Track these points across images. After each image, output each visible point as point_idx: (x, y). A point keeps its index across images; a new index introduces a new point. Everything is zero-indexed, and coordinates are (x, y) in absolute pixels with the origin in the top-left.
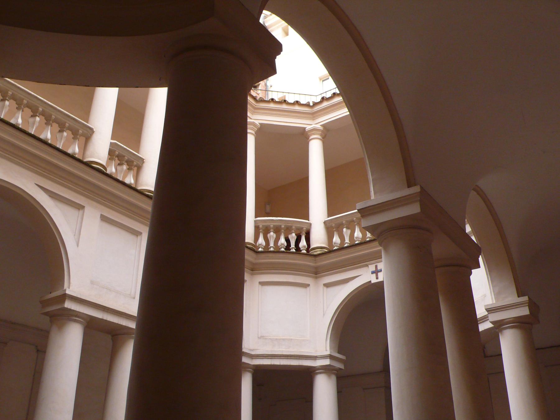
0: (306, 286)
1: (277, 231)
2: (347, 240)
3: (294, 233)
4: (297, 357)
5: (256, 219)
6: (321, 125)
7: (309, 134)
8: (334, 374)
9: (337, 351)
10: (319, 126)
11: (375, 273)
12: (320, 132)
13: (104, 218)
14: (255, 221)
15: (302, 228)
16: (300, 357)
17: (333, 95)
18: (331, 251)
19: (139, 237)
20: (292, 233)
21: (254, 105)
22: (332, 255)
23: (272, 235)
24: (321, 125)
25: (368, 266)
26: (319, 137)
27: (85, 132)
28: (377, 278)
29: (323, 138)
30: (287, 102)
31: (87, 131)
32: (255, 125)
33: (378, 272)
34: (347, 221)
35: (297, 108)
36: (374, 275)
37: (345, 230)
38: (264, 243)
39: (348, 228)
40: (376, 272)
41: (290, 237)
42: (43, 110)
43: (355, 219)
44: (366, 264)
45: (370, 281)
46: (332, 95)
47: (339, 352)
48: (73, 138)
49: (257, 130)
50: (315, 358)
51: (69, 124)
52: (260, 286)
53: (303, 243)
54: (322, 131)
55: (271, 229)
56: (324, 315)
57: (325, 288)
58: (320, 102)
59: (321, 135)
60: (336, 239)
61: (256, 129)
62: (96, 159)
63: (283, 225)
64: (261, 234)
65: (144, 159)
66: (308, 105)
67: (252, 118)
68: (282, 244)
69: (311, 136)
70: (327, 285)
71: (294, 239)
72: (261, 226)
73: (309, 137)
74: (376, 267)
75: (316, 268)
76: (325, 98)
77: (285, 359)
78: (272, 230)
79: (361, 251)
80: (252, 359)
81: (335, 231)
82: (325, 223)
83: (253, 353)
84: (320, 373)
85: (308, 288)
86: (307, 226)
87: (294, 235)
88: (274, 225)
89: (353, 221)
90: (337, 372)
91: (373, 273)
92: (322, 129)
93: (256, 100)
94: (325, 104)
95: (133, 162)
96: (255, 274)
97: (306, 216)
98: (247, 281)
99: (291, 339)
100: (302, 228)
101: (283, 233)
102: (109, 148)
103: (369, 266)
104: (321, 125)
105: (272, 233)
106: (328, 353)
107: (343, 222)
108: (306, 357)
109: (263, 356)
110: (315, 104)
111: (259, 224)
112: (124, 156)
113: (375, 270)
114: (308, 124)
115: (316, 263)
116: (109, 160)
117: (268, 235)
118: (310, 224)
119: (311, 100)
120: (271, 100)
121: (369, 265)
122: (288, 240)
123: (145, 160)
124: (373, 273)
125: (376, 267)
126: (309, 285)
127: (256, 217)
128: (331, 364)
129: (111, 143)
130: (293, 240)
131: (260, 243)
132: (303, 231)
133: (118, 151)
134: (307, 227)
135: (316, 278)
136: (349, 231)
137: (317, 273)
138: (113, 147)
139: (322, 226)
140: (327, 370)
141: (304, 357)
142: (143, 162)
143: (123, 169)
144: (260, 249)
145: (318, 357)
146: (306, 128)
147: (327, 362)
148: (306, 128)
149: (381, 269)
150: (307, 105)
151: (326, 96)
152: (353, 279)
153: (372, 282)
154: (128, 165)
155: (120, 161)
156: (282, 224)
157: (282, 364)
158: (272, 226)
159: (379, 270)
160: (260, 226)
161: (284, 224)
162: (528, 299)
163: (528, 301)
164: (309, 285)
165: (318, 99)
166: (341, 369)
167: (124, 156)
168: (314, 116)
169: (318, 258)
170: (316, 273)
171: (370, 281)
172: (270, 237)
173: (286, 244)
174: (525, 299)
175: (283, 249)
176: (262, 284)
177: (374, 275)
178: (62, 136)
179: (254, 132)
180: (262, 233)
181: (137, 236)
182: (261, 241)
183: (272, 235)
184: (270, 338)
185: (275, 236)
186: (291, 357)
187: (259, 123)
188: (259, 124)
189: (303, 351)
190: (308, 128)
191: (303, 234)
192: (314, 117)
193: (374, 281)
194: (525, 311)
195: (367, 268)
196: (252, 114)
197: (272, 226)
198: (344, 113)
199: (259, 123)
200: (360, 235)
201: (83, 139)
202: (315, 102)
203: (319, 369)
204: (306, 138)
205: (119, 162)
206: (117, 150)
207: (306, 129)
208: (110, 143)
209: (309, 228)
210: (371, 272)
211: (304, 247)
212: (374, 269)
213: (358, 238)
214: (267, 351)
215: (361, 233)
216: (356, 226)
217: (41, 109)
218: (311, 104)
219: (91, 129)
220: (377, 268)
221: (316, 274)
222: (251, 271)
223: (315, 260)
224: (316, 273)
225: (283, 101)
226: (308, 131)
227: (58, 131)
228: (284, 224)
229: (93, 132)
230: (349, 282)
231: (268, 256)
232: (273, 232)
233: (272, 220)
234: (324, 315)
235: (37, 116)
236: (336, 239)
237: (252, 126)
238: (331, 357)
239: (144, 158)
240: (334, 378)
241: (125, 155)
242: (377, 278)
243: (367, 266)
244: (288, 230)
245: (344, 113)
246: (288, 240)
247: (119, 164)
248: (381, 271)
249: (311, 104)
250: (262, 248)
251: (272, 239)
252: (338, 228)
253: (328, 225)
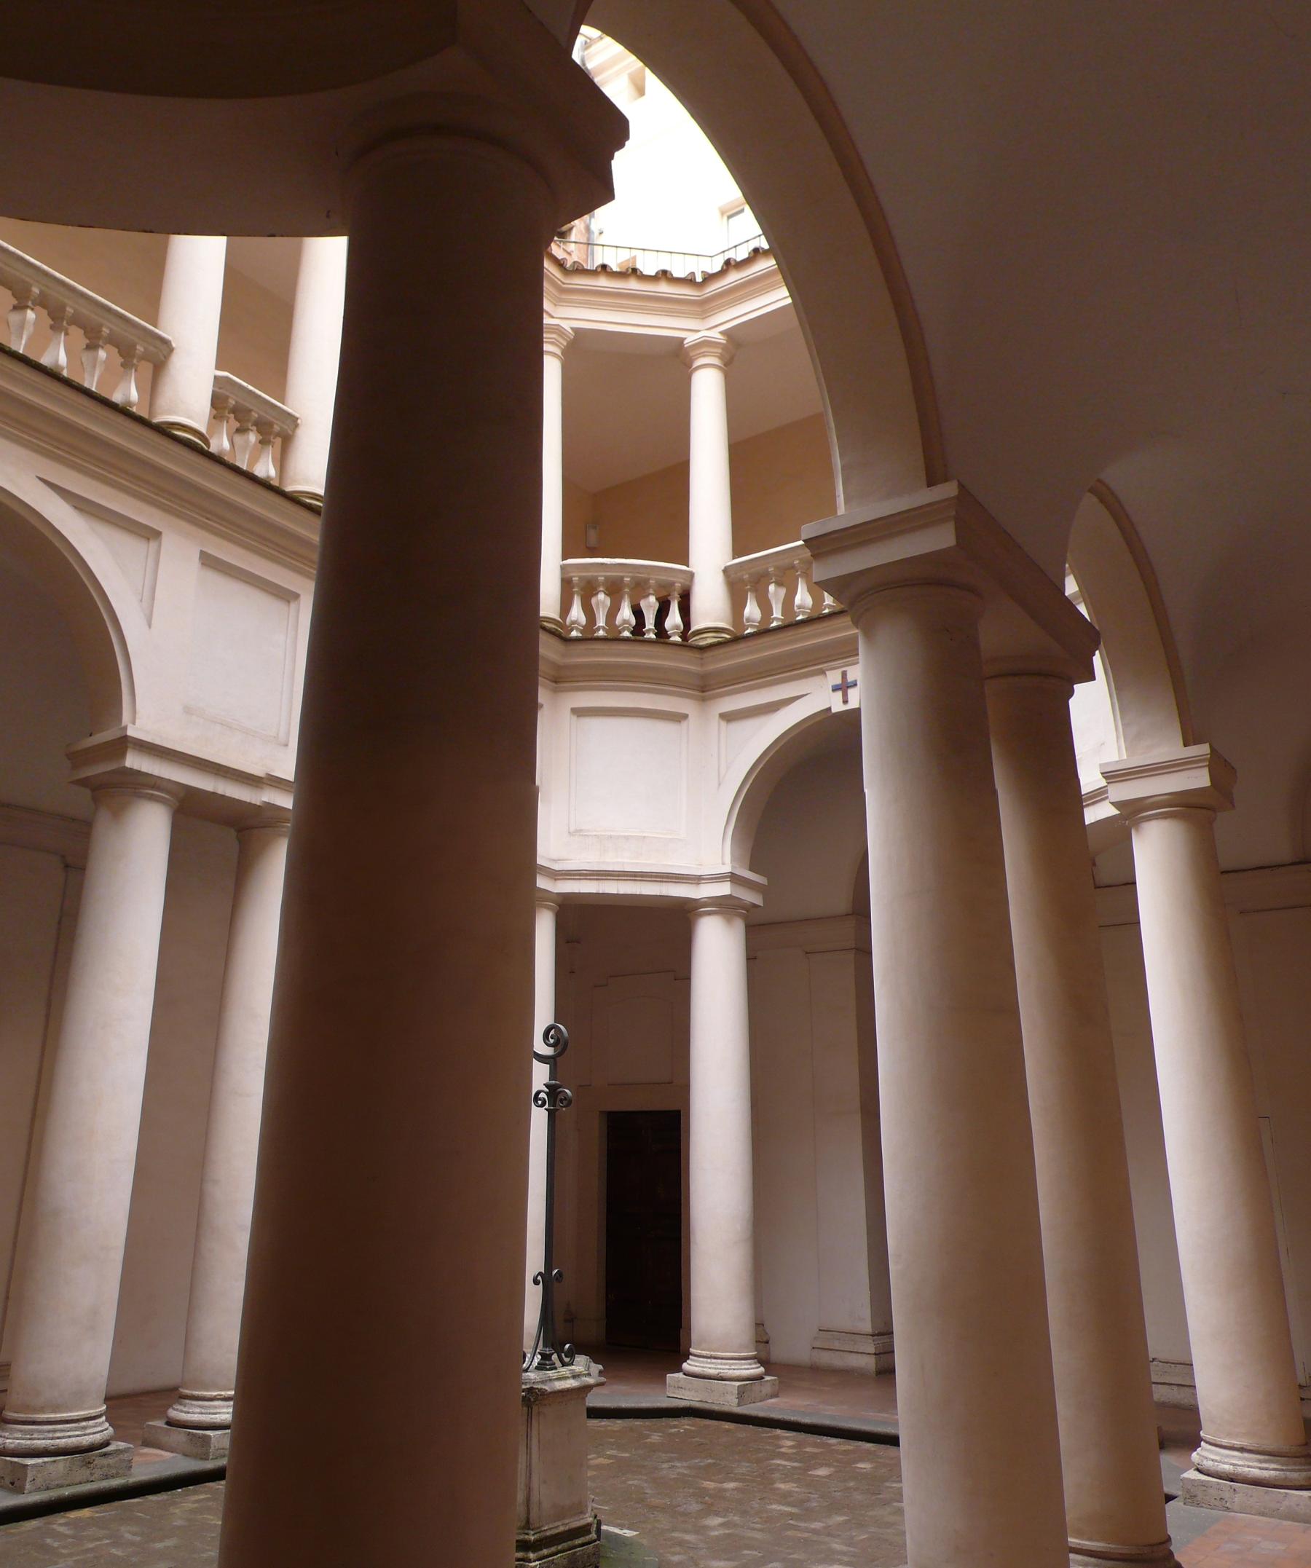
0: (679, 718)
1: (614, 590)
2: (777, 613)
3: (652, 594)
4: (656, 877)
5: (565, 562)
6: (721, 333)
7: (691, 354)
8: (740, 915)
9: (748, 867)
10: (715, 335)
12: (720, 351)
13: (208, 561)
14: (563, 568)
15: (672, 584)
16: (662, 877)
17: (752, 253)
18: (738, 639)
19: (293, 605)
20: (647, 596)
21: (559, 282)
22: (741, 646)
23: (602, 600)
24: (722, 333)
25: (825, 674)
26: (715, 361)
27: (151, 348)
29: (725, 365)
30: (638, 273)
31: (155, 347)
32: (563, 333)
34: (777, 568)
35: (664, 288)
36: (839, 694)
37: (772, 588)
38: (583, 620)
39: (779, 584)
41: (643, 604)
42: (41, 292)
43: (797, 562)
44: (821, 669)
45: (829, 709)
46: (749, 253)
47: (752, 868)
48: (122, 365)
49: (567, 344)
50: (697, 880)
51: (111, 330)
52: (574, 718)
53: (674, 619)
54: (724, 347)
55: (599, 586)
56: (719, 784)
57: (723, 724)
58: (719, 271)
59: (721, 357)
60: (752, 610)
61: (565, 344)
62: (181, 416)
63: (627, 577)
64: (576, 596)
65: (297, 419)
66: (691, 280)
67: (555, 316)
68: (625, 622)
69: (697, 359)
70: (728, 717)
71: (653, 608)
72: (577, 579)
73: (692, 362)
75: (704, 677)
76: (733, 263)
77: (629, 882)
78: (601, 589)
79: (807, 638)
80: (556, 880)
81: (750, 590)
82: (726, 571)
83: (557, 867)
84: (709, 913)
85: (684, 724)
86: (684, 579)
87: (652, 599)
88: (605, 577)
89: (793, 567)
90: (747, 911)
91: (835, 689)
92: (725, 342)
93: (565, 269)
94: (734, 277)
95: (271, 425)
96: (562, 691)
97: (682, 555)
98: (544, 706)
99: (644, 837)
100: (672, 584)
101: (626, 596)
102: (213, 391)
103: (827, 673)
104: (721, 333)
105: (601, 596)
106: (727, 868)
107: (767, 568)
108: (676, 878)
109: (580, 875)
110: (709, 278)
111: (572, 574)
112: (250, 411)
113: (840, 682)
114: (690, 330)
115: (702, 665)
116: (214, 421)
117: (593, 601)
118: (692, 575)
119: (700, 267)
120: (599, 269)
121: (828, 670)
122: (638, 613)
123: (299, 421)
124: (835, 689)
125: (844, 675)
126: (685, 717)
127: (564, 559)
128: (733, 894)
129: (216, 378)
130: (652, 612)
131: (573, 619)
132: (675, 590)
133: (234, 397)
134: (682, 581)
135: (704, 700)
136: (782, 592)
137: (704, 688)
138: (220, 388)
139: (720, 578)
140: (724, 906)
141: (672, 878)
142: (297, 426)
143: (247, 441)
144: (574, 634)
145: (704, 879)
146: (685, 338)
147: (724, 889)
148: (685, 338)
150: (689, 281)
151: (734, 258)
152: (789, 704)
153: (834, 710)
154: (259, 431)
155: (239, 422)
156: (627, 574)
157: (622, 892)
158: (601, 579)
159: (850, 682)
160: (574, 579)
161: (630, 574)
164: (685, 717)
165: (716, 266)
166: (755, 906)
167: (250, 411)
168: (704, 308)
169: (708, 654)
170: (703, 689)
171: (829, 709)
172: (598, 604)
173: (633, 621)
175: (626, 634)
176: (579, 712)
178: (95, 359)
179: (558, 352)
180: (578, 595)
181: (289, 602)
182: (577, 613)
183: (602, 600)
184: (595, 833)
185: (608, 601)
186: (642, 876)
187: (572, 328)
188: (570, 331)
189: (669, 863)
190: (690, 339)
191: (674, 599)
192: (704, 312)
196: (555, 305)
197: (601, 579)
198: (777, 301)
199: (572, 328)
200: (809, 601)
201: (147, 368)
202: (708, 274)
203: (705, 905)
204: (685, 364)
205: (237, 425)
206: (231, 395)
207: (685, 342)
208: (213, 378)
209: (687, 583)
211: (677, 627)
212: (839, 681)
213: (804, 608)
214: (588, 862)
215: (812, 597)
216: (800, 579)
217: (36, 290)
218: (699, 279)
219: (166, 343)
220: (846, 678)
221: (703, 692)
222: (554, 685)
223: (702, 659)
224: (703, 689)
225: (630, 270)
226: (690, 346)
227: (85, 347)
228: (630, 574)
229: (171, 350)
230: (779, 709)
231: (593, 649)
232: (605, 593)
233: (602, 564)
234: (719, 784)
235: (27, 307)
236: (752, 610)
237: (554, 336)
238: (733, 878)
239: (297, 415)
240: (739, 926)
241: (251, 407)
243: (822, 672)
244: (640, 588)
245: (777, 301)
246: (638, 613)
247: (238, 431)
249: (699, 279)
250: (577, 629)
251: (601, 609)
252: (757, 583)
253: (733, 576)
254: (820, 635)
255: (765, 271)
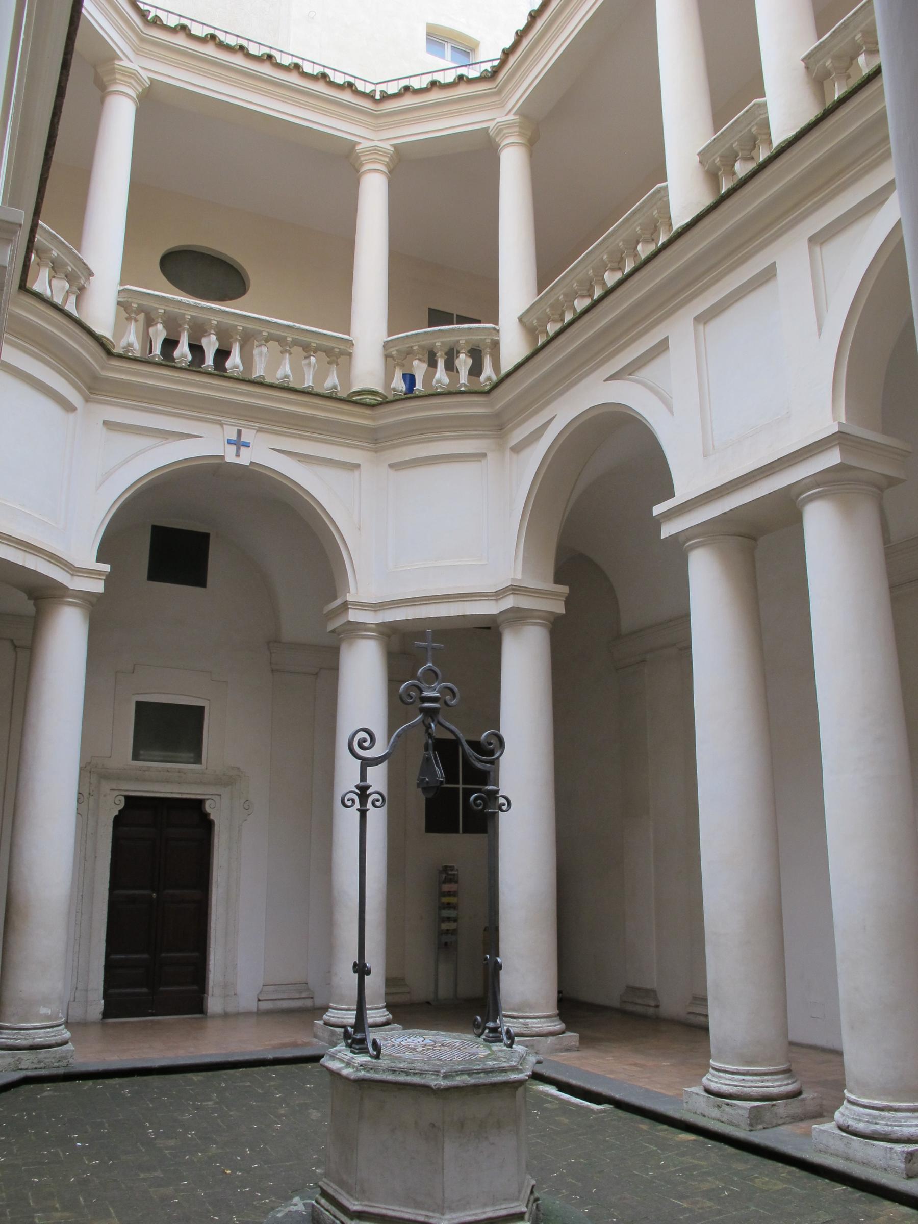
6: (149, 78)
10: (145, 75)
11: (235, 444)
25: (222, 427)
28: (238, 455)
33: (242, 445)
36: (234, 447)
40: (239, 443)
44: (220, 421)
45: (223, 457)
74: (239, 433)
91: (230, 442)
94: (180, 40)
103: (225, 426)
104: (149, 78)
124: (230, 442)
125: (239, 433)
149: (249, 443)
153: (227, 460)
162: (568, 592)
163: (567, 595)
169: (115, 363)
171: (223, 457)
174: (565, 589)
177: (234, 447)
193: (231, 458)
194: (559, 608)
195: (218, 427)
210: (228, 440)
212: (234, 437)
230: (167, 439)
242: (238, 455)
243: (222, 425)
248: (249, 446)
254: (348, 414)
255: (210, 58)
